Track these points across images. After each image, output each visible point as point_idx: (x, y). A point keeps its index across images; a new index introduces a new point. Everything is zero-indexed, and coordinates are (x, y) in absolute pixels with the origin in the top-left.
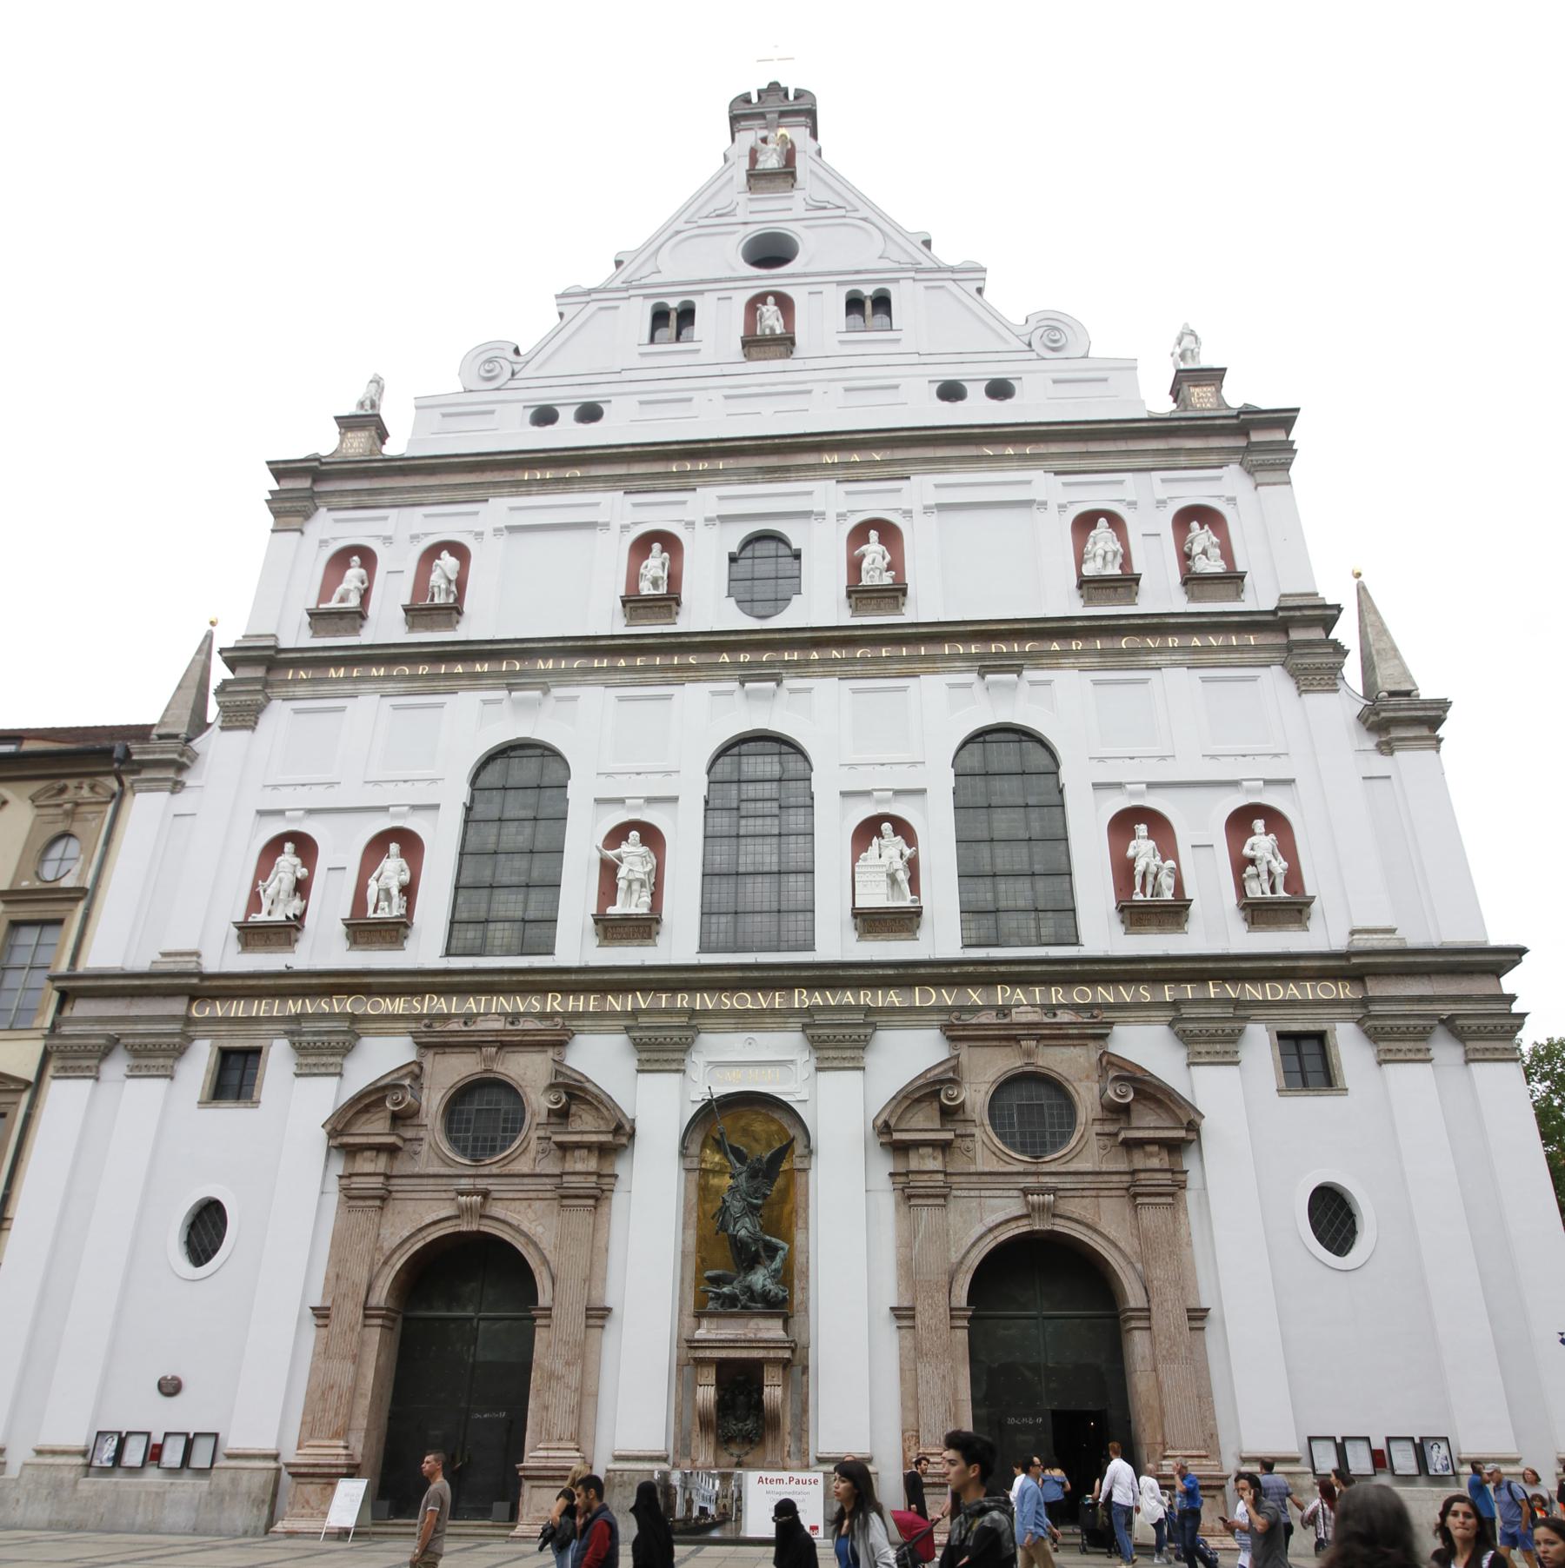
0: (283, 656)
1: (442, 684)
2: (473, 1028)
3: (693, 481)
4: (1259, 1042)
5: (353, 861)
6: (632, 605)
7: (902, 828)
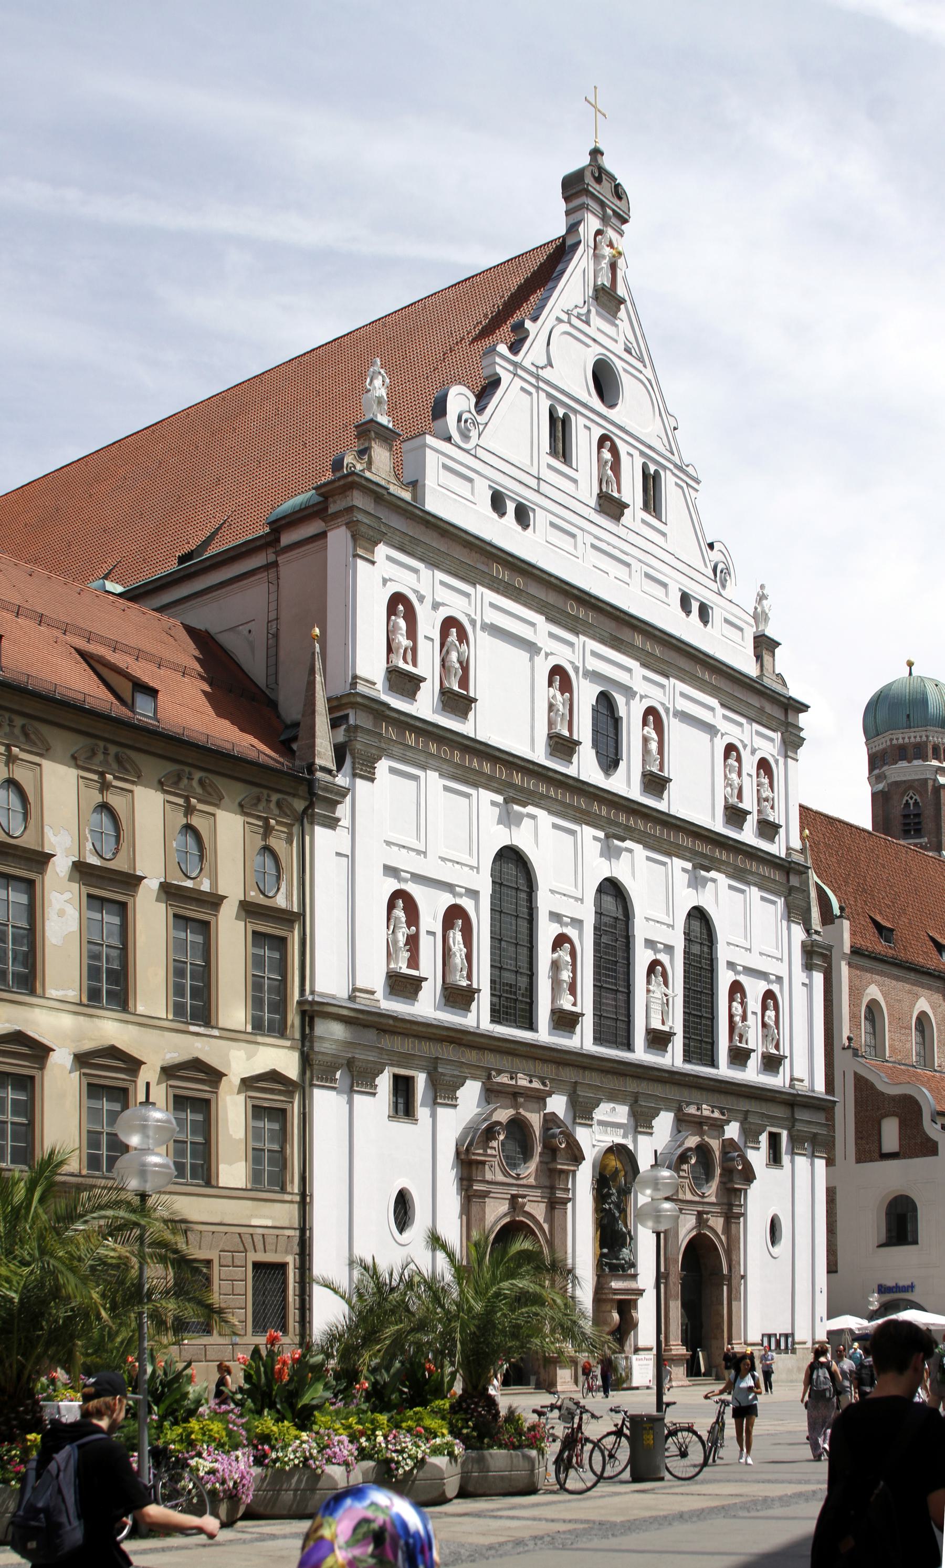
0: (388, 712)
1: (472, 777)
2: (513, 1082)
3: (580, 628)
4: (764, 1138)
5: (438, 929)
6: (557, 739)
7: (664, 975)
